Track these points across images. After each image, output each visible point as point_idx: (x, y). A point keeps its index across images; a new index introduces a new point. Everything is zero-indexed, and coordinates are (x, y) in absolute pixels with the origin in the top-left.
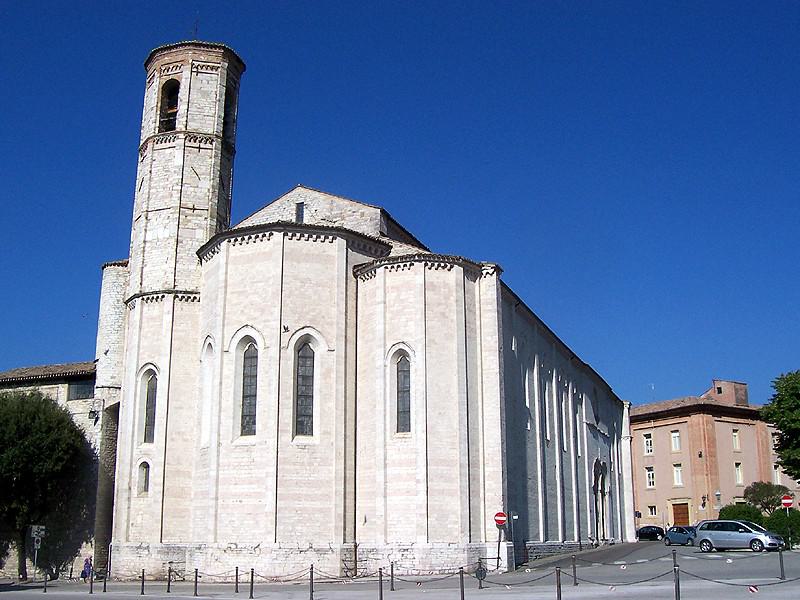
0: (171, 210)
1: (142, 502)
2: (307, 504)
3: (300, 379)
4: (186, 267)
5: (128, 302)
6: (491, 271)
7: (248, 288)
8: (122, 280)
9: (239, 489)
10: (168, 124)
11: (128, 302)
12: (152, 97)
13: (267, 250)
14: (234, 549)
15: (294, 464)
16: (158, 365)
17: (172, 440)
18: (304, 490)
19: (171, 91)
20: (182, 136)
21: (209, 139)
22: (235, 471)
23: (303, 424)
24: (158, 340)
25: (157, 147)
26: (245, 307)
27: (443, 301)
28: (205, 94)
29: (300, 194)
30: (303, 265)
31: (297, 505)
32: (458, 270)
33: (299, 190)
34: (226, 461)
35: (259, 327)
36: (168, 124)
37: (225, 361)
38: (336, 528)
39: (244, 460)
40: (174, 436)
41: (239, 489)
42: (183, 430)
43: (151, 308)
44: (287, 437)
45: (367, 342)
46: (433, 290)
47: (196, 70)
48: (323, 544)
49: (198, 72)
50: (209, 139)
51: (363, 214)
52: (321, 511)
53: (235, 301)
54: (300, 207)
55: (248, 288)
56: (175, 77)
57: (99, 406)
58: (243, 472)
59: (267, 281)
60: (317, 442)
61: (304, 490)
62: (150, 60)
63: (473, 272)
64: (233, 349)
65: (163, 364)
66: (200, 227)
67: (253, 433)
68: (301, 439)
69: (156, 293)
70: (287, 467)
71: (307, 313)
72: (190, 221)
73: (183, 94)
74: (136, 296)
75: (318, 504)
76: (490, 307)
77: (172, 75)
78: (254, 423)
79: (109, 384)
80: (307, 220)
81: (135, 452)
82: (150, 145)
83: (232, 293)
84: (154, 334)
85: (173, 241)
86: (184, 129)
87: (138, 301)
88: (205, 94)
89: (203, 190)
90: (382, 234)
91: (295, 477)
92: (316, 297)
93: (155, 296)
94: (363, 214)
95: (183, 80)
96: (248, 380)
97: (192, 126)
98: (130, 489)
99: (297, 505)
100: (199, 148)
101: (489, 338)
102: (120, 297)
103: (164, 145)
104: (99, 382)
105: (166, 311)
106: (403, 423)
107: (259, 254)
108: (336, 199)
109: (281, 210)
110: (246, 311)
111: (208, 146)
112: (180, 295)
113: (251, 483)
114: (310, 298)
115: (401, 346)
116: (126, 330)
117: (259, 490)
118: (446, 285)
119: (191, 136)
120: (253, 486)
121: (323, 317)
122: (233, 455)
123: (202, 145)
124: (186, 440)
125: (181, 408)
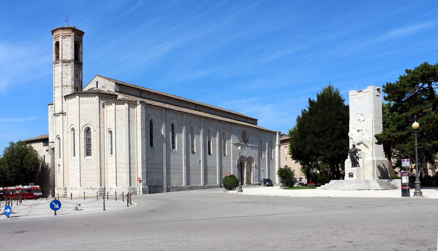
2: (89, 176)
20: (61, 62)
21: (70, 62)
23: (88, 153)
28: (67, 46)
31: (87, 176)
38: (97, 182)
44: (83, 157)
47: (64, 37)
48: (94, 187)
50: (70, 62)
52: (93, 178)
63: (132, 104)
64: (70, 132)
75: (92, 176)
88: (67, 46)
90: (116, 91)
97: (64, 58)
99: (87, 176)
111: (70, 64)
118: (122, 109)
119: (64, 62)
123: (68, 64)
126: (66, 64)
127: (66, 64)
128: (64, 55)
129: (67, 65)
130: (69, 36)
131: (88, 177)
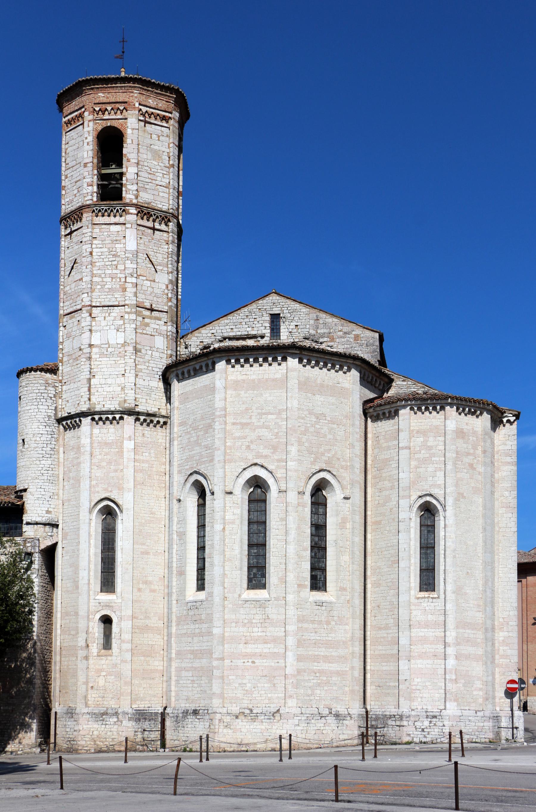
0: (127, 309)
1: (103, 662)
2: (325, 666)
3: (314, 529)
4: (146, 383)
5: (69, 421)
7: (254, 420)
8: (52, 391)
9: (250, 648)
10: (110, 191)
11: (69, 421)
12: (79, 147)
14: (250, 714)
15: (313, 622)
17: (139, 590)
18: (322, 652)
19: (110, 145)
21: (165, 217)
22: (245, 629)
23: (318, 581)
25: (100, 220)
26: (252, 442)
27: (472, 451)
29: (274, 303)
30: (318, 397)
31: (316, 666)
32: (486, 418)
33: (274, 298)
34: (233, 617)
35: (270, 467)
36: (110, 191)
37: (228, 505)
39: (257, 617)
40: (141, 586)
41: (250, 648)
42: (150, 579)
43: (105, 431)
45: (380, 491)
46: (463, 438)
51: (357, 337)
53: (237, 434)
54: (275, 319)
55: (254, 420)
58: (256, 629)
59: (279, 413)
60: (333, 599)
61: (322, 652)
65: (125, 499)
66: (160, 334)
68: (318, 595)
69: (112, 413)
71: (323, 454)
72: (147, 325)
74: (83, 414)
75: (334, 667)
76: (509, 459)
78: (264, 576)
79: (44, 520)
81: (92, 603)
82: (87, 216)
83: (234, 424)
84: (109, 463)
85: (130, 349)
86: (135, 201)
89: (160, 286)
91: (313, 636)
92: (331, 437)
93: (110, 417)
94: (357, 337)
98: (88, 646)
99: (316, 666)
100: (154, 229)
101: (507, 493)
102: (52, 413)
103: (106, 219)
104: (26, 518)
106: (428, 580)
107: (267, 380)
108: (323, 315)
110: (252, 447)
111: (163, 227)
112: (142, 418)
113: (265, 643)
114: (325, 436)
115: (428, 499)
116: (61, 455)
117: (276, 650)
118: (475, 433)
120: (269, 646)
121: (338, 459)
122: (242, 611)
123: (157, 226)
124: (154, 591)
125: (147, 553)
126: (150, 224)
127: (150, 224)
131: (322, 672)
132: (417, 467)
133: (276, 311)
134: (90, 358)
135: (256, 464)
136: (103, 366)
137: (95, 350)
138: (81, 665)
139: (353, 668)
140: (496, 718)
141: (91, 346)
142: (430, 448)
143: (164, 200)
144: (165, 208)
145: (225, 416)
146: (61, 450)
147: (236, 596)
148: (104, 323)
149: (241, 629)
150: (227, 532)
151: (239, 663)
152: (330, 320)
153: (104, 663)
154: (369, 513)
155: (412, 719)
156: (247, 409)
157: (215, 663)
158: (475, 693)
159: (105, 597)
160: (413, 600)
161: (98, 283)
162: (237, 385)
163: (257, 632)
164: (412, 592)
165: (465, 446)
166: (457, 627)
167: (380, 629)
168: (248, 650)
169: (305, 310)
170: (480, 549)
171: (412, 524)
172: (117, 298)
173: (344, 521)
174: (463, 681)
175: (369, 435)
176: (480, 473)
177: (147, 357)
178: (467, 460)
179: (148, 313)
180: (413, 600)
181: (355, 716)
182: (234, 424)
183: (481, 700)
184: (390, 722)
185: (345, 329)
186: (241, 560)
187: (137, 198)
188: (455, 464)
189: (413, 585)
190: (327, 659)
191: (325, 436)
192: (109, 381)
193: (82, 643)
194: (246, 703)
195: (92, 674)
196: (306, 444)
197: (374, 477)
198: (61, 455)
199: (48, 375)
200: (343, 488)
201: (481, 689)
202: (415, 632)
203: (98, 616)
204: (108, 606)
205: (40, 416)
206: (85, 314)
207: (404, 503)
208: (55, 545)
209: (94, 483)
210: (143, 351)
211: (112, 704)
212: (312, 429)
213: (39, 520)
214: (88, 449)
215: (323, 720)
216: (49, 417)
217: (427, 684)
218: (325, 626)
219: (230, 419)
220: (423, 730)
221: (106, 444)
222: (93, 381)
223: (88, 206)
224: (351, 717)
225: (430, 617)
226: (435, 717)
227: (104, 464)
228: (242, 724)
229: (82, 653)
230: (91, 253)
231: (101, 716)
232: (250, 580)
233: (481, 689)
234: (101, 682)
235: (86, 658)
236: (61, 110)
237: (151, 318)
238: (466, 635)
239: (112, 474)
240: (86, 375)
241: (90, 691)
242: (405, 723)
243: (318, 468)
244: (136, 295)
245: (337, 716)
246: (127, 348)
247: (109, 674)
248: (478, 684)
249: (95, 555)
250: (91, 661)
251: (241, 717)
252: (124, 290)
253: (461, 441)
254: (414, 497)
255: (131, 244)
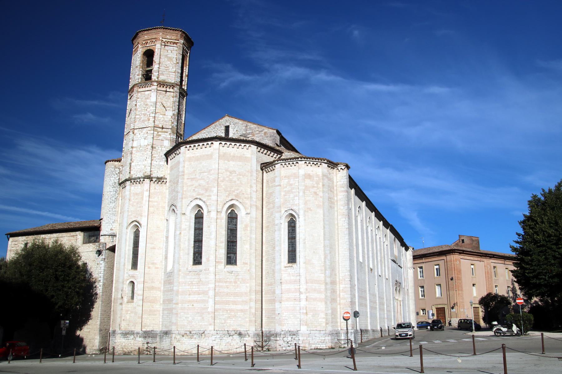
0: (149, 129)
1: (129, 306)
2: (233, 307)
3: (229, 231)
4: (158, 163)
5: (122, 184)
6: (343, 167)
7: (197, 176)
8: (118, 171)
9: (192, 297)
10: (147, 76)
11: (122, 184)
12: (137, 59)
13: (209, 153)
14: (190, 334)
15: (226, 282)
16: (141, 223)
17: (149, 268)
18: (232, 299)
19: (149, 55)
21: (172, 86)
22: (189, 287)
23: (231, 259)
24: (140, 207)
25: (140, 90)
26: (196, 187)
27: (316, 185)
28: (170, 59)
29: (226, 120)
30: (231, 162)
31: (227, 307)
33: (227, 118)
35: (204, 200)
36: (147, 76)
39: (195, 280)
40: (150, 266)
41: (192, 297)
42: (155, 262)
43: (136, 188)
45: (269, 209)
46: (310, 178)
49: (165, 45)
50: (172, 86)
51: (265, 133)
52: (242, 311)
53: (189, 184)
54: (227, 128)
55: (197, 176)
56: (151, 48)
57: (103, 247)
58: (194, 287)
59: (209, 172)
61: (232, 299)
62: (135, 37)
65: (143, 221)
66: (167, 139)
67: (200, 263)
68: (231, 268)
69: (139, 178)
70: (221, 284)
71: (234, 191)
72: (160, 135)
73: (156, 58)
74: (126, 180)
75: (239, 307)
76: (343, 189)
77: (150, 46)
78: (201, 257)
79: (109, 233)
80: (231, 135)
81: (126, 275)
82: (135, 89)
83: (188, 179)
84: (138, 203)
85: (150, 147)
86: (157, 80)
87: (128, 183)
88: (170, 59)
89: (168, 117)
91: (226, 290)
92: (239, 182)
93: (139, 180)
94: (265, 133)
95: (156, 50)
96: (197, 232)
97: (162, 78)
98: (122, 297)
99: (227, 307)
100: (166, 91)
101: (342, 208)
102: (117, 181)
103: (144, 89)
104: (101, 233)
105: (145, 189)
107: (204, 156)
108: (249, 124)
109: (217, 129)
110: (196, 190)
111: (171, 90)
112: (154, 180)
113: (199, 294)
114: (235, 182)
115: (291, 212)
116: (120, 201)
117: (204, 298)
118: (317, 176)
119: (162, 84)
120: (201, 296)
121: (243, 194)
122: (188, 277)
123: (168, 90)
124: (157, 268)
125: (154, 248)
126: (164, 89)
127: (164, 89)
128: (163, 74)
129: (166, 91)
130: (174, 43)
131: (231, 310)
132: (285, 195)
133: (227, 124)
134: (131, 153)
135: (197, 198)
136: (137, 156)
137: (134, 149)
138: (119, 307)
139: (250, 308)
140: (337, 334)
141: (132, 147)
142: (291, 185)
143: (173, 78)
144: (173, 82)
145: (183, 175)
146: (120, 198)
147: (185, 269)
148: (139, 136)
149: (187, 287)
150: (182, 235)
151: (186, 305)
152: (253, 126)
153: (130, 305)
154: (264, 222)
155: (282, 336)
156: (194, 171)
157: (174, 306)
158: (320, 320)
159: (133, 272)
160: (283, 268)
161: (138, 118)
162: (190, 159)
163: (195, 288)
164: (282, 264)
165: (311, 182)
166: (307, 283)
167: (269, 285)
168: (190, 299)
169: (241, 122)
170: (322, 238)
171: (282, 226)
172: (146, 124)
173: (246, 226)
174: (312, 314)
175: (264, 181)
176: (321, 197)
177: (159, 151)
178: (313, 190)
179: (160, 130)
180: (283, 268)
181: (251, 335)
182: (188, 179)
183: (324, 324)
184: (272, 338)
185: (260, 130)
186: (189, 249)
187: (158, 78)
188: (304, 192)
189: (282, 260)
190: (235, 303)
191: (235, 182)
192: (139, 163)
193: (120, 296)
194: (189, 328)
195: (124, 312)
196: (224, 187)
197: (267, 203)
198: (120, 201)
199: (116, 163)
200: (245, 208)
201: (324, 318)
202: (284, 286)
203: (128, 282)
204: (133, 277)
205: (111, 183)
206: (131, 133)
207: (277, 215)
208: (115, 245)
209: (130, 214)
210: (157, 148)
211: (132, 329)
212: (227, 179)
213: (106, 233)
214: (128, 197)
215: (231, 337)
216: (115, 183)
217: (291, 316)
218: (234, 284)
219: (186, 177)
220: (288, 343)
221: (137, 194)
222: (132, 164)
223: (136, 84)
224: (249, 336)
225: (292, 278)
226: (294, 335)
227: (135, 204)
228: (185, 340)
229: (120, 301)
230: (136, 105)
231: (126, 334)
232: (194, 260)
233: (324, 318)
234: (128, 317)
235: (121, 304)
236: (133, 44)
237: (162, 132)
238: (314, 287)
239: (138, 209)
240: (129, 161)
241: (123, 322)
242: (278, 339)
243: (230, 199)
244: (154, 122)
245: (240, 334)
246: (148, 147)
247: (132, 312)
248: (322, 315)
249: (129, 250)
250: (124, 306)
251: (185, 336)
252: (149, 120)
253: (309, 180)
254: (283, 212)
255: (153, 99)
